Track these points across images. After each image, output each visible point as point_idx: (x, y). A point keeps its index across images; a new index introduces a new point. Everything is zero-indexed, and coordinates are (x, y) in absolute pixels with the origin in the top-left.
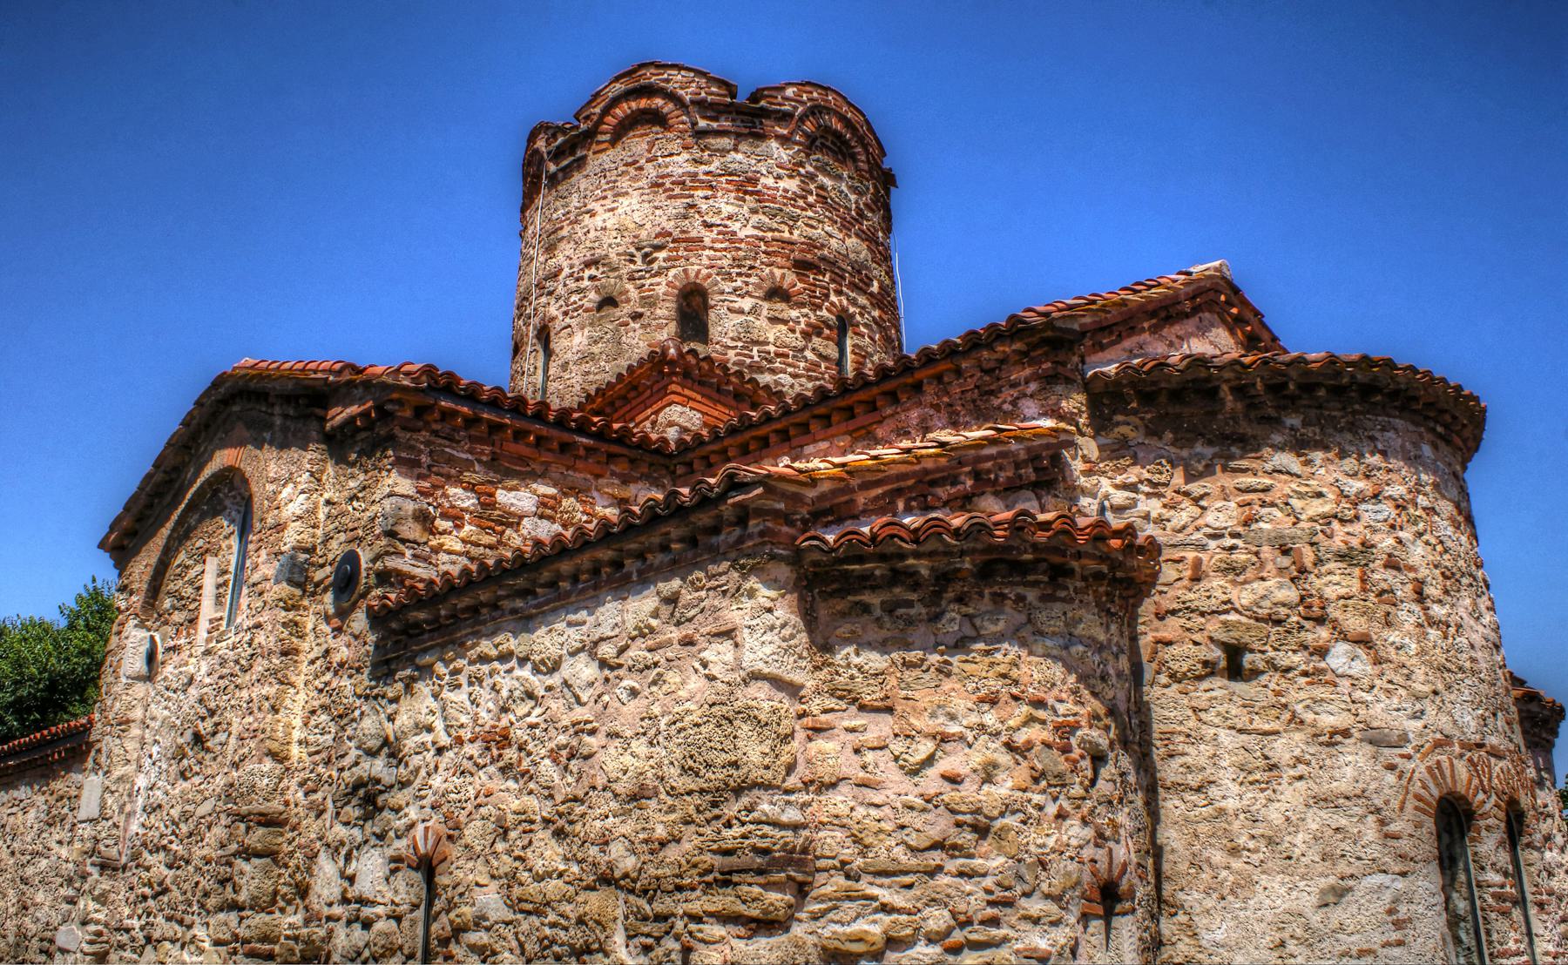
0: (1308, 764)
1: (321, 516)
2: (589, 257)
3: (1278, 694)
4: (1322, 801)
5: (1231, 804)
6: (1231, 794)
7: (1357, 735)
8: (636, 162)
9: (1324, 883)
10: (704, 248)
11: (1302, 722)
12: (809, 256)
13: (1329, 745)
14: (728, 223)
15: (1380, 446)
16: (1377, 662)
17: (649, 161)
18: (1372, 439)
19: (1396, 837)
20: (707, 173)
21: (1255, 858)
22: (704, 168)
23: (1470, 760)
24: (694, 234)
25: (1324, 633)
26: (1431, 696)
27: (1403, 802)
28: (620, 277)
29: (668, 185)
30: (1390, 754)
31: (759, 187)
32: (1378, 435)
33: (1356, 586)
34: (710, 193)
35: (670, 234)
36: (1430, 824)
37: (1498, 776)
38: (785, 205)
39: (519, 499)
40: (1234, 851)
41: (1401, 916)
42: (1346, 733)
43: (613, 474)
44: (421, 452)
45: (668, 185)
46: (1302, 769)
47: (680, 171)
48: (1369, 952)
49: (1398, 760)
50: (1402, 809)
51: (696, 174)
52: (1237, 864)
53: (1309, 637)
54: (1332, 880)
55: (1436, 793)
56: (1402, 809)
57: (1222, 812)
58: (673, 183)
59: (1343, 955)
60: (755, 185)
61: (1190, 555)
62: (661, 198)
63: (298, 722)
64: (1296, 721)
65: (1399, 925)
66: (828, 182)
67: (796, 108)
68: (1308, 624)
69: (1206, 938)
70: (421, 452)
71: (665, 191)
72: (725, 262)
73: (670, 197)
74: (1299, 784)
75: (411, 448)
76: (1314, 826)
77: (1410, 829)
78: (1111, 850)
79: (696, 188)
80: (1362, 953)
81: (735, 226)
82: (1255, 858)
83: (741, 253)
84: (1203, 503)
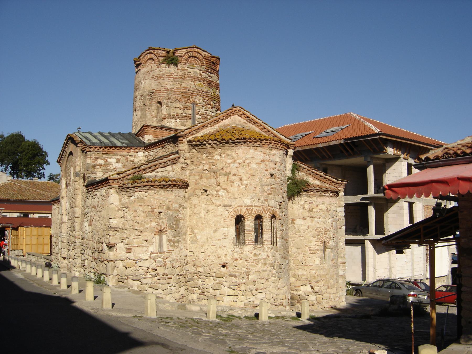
0: (213, 210)
1: (82, 165)
2: (141, 94)
3: (211, 198)
4: (216, 216)
5: (203, 216)
6: (202, 215)
7: (222, 205)
8: (149, 72)
9: (214, 229)
10: (161, 92)
11: (214, 203)
12: (184, 91)
13: (218, 207)
14: (166, 86)
15: (237, 153)
16: (228, 192)
17: (151, 71)
18: (235, 151)
19: (226, 222)
20: (162, 74)
21: (205, 225)
22: (161, 73)
23: (247, 209)
24: (159, 89)
25: (219, 187)
26: (239, 198)
27: (229, 216)
28: (146, 100)
29: (154, 77)
30: (228, 208)
31: (173, 76)
32: (236, 150)
33: (226, 179)
34: (163, 79)
35: (154, 89)
36: (234, 220)
37: (255, 211)
38: (179, 79)
39: (112, 160)
40: (202, 224)
41: (226, 234)
42: (220, 205)
43: (132, 152)
44: (92, 155)
45: (154, 77)
46: (213, 211)
47: (157, 74)
48: (220, 240)
49: (229, 210)
50: (228, 217)
51: (160, 74)
52: (202, 226)
53: (216, 189)
54: (216, 229)
55: (236, 214)
56: (228, 217)
57: (201, 217)
58: (155, 77)
59: (216, 240)
60: (172, 76)
61: (201, 174)
62: (153, 81)
63: (81, 201)
64: (213, 203)
65: (225, 236)
66: (190, 70)
67: (182, 54)
68: (216, 186)
69: (198, 237)
70: (92, 155)
71: (154, 79)
72: (165, 95)
73: (155, 80)
74: (212, 214)
75: (90, 155)
76: (214, 220)
77: (229, 221)
78: (161, 226)
79: (160, 78)
80: (219, 240)
81: (168, 86)
82: (205, 225)
83: (169, 93)
84: (204, 165)
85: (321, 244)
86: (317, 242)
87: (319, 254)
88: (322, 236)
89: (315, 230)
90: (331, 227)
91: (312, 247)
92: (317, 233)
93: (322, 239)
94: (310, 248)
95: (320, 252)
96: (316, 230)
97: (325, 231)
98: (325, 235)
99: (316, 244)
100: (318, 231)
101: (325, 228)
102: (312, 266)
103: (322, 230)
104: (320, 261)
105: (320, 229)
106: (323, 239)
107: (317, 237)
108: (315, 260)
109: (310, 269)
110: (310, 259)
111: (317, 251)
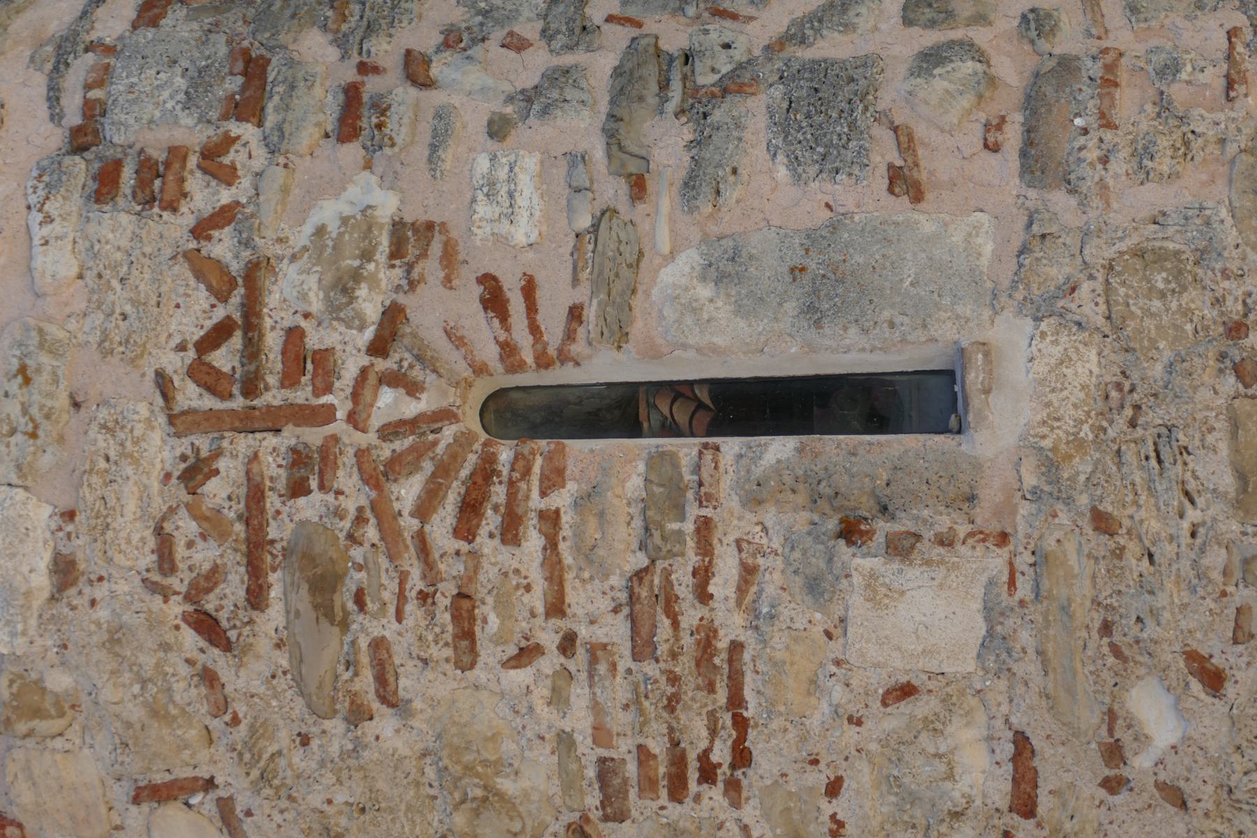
85: (510, 533)
86: (491, 621)
87: (748, 572)
88: (347, 478)
89: (216, 658)
90: (177, 226)
91: (601, 734)
92: (274, 616)
93: (407, 492)
94: (606, 770)
95: (705, 528)
96: (207, 625)
97: (251, 387)
98: (339, 400)
99: (526, 654)
100: (234, 587)
101: (191, 396)
102: (1022, 743)
103: (216, 490)
104: (901, 548)
105: (186, 527)
106: (396, 467)
107: (367, 628)
108: (879, 682)
109: (1090, 790)
110: (860, 778)
111: (691, 615)
